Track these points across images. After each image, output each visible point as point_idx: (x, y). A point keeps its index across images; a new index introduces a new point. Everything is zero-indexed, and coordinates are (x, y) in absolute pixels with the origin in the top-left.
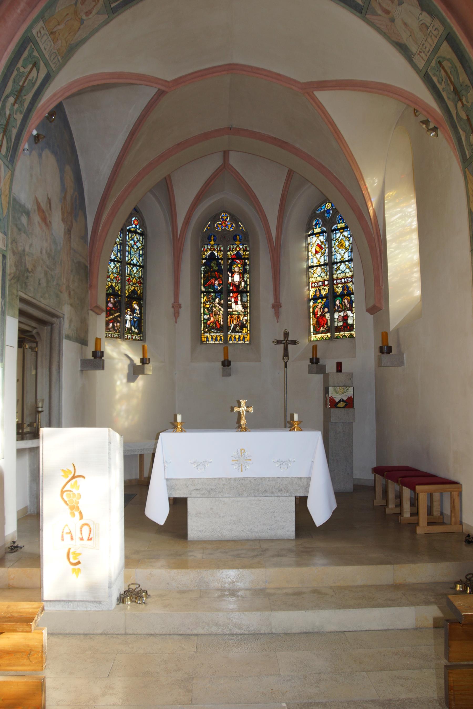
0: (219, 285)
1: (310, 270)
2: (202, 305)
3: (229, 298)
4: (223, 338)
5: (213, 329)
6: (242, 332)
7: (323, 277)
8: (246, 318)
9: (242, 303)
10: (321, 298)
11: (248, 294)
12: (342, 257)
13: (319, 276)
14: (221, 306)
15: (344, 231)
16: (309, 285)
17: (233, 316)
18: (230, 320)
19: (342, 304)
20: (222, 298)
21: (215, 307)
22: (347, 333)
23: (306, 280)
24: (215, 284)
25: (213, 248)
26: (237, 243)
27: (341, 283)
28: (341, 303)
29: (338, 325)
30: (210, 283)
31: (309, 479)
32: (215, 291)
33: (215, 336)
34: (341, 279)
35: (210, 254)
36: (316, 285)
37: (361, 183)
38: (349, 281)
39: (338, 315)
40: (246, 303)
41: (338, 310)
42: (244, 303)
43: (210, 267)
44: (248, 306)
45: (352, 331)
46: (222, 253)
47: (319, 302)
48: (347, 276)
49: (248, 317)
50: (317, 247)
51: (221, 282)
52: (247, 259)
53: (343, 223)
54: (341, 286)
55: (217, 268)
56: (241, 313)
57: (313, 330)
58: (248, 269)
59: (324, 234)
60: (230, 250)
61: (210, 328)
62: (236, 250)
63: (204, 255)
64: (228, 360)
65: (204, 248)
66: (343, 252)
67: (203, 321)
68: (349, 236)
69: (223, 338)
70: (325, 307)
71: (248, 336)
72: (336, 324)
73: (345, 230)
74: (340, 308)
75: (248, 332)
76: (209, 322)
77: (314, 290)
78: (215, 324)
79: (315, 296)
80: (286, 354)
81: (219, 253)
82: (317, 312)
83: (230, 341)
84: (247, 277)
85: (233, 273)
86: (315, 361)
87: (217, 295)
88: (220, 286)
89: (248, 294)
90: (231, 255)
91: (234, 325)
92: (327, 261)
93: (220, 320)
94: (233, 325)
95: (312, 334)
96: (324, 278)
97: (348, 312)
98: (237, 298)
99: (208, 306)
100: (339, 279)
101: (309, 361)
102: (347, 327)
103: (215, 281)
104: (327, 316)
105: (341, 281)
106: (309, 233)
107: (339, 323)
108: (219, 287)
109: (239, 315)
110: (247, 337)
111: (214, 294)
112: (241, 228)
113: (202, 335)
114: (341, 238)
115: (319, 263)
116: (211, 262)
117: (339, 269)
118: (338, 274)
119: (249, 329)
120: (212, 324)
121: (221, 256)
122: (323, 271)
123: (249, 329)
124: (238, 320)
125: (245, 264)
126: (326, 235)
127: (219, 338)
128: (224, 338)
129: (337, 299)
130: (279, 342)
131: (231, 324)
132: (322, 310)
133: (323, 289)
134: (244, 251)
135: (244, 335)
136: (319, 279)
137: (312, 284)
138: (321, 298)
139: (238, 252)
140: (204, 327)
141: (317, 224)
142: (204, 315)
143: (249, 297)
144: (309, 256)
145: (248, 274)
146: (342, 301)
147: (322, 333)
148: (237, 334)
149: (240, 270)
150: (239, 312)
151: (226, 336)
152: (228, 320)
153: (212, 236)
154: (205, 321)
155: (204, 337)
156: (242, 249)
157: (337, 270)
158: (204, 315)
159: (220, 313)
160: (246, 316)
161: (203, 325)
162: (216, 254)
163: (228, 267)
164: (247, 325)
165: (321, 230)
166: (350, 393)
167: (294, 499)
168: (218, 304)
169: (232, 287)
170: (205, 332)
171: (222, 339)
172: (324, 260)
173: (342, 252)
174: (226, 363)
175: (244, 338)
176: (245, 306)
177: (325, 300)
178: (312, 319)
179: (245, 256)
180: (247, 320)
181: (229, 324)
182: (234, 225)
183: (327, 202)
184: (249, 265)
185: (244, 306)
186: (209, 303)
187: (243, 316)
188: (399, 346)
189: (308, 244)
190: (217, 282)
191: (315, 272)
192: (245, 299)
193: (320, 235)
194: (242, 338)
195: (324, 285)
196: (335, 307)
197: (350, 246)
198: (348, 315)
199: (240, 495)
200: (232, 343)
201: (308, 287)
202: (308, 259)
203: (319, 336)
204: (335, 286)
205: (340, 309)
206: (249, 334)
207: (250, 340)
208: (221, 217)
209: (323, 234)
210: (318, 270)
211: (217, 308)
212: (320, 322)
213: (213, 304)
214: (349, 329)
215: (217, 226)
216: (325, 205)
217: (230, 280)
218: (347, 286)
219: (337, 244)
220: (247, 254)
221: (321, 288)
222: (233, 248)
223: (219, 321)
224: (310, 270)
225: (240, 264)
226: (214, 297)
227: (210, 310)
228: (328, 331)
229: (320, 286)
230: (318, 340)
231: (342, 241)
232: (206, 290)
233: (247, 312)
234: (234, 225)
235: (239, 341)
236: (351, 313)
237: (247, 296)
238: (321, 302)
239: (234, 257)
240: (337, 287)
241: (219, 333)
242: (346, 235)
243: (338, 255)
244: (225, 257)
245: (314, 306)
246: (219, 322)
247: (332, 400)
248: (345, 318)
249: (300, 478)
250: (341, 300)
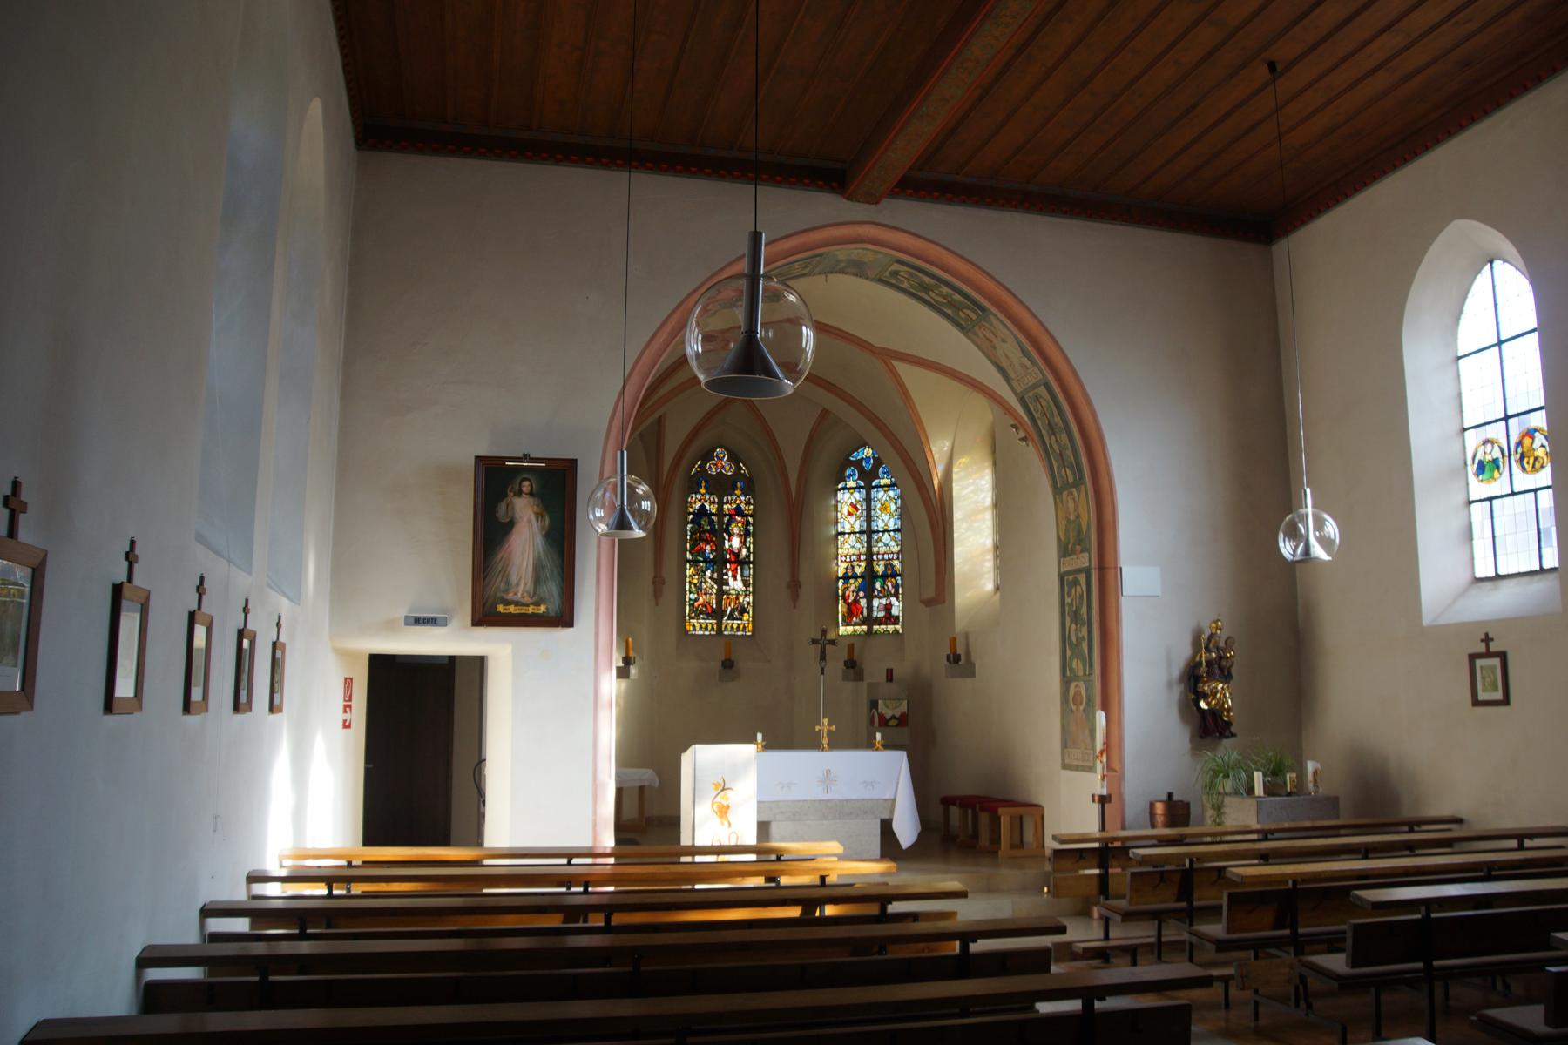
0: (712, 552)
1: (839, 537)
2: (688, 580)
3: (724, 571)
4: (715, 627)
5: (702, 613)
8: (747, 599)
10: (855, 577)
11: (751, 566)
12: (886, 525)
13: (853, 547)
15: (889, 490)
16: (837, 559)
21: (705, 582)
22: (891, 628)
27: (883, 559)
28: (882, 586)
31: (894, 800)
32: (706, 561)
35: (700, 507)
37: (927, 450)
43: (700, 525)
45: (898, 624)
49: (750, 599)
51: (714, 548)
52: (751, 516)
55: (709, 528)
57: (843, 620)
60: (727, 503)
62: (735, 503)
64: (730, 660)
69: (715, 627)
70: (859, 590)
71: (750, 625)
72: (875, 614)
76: (696, 604)
77: (844, 565)
78: (706, 606)
79: (846, 573)
80: (823, 657)
82: (849, 596)
85: (731, 535)
86: (851, 664)
89: (751, 566)
90: (728, 509)
92: (865, 528)
95: (841, 625)
99: (695, 581)
101: (843, 663)
102: (889, 618)
104: (863, 602)
106: (840, 486)
109: (738, 594)
114: (884, 498)
117: (881, 541)
121: (714, 511)
122: (859, 541)
125: (748, 522)
126: (864, 491)
127: (710, 627)
130: (814, 642)
132: (855, 594)
134: (746, 504)
136: (852, 551)
137: (842, 556)
138: (855, 577)
139: (738, 505)
140: (690, 610)
141: (851, 475)
146: (885, 583)
147: (855, 624)
149: (740, 531)
151: (719, 624)
154: (691, 602)
157: (877, 541)
158: (690, 593)
161: (688, 608)
162: (708, 507)
166: (904, 708)
167: (878, 822)
168: (710, 578)
170: (691, 618)
173: (886, 517)
174: (728, 664)
175: (744, 627)
177: (860, 580)
180: (748, 603)
182: (733, 467)
186: (697, 577)
188: (968, 653)
189: (837, 502)
190: (708, 548)
192: (746, 573)
194: (741, 627)
195: (859, 560)
199: (825, 818)
202: (837, 522)
203: (850, 629)
204: (875, 563)
207: (753, 631)
212: (852, 609)
215: (710, 467)
217: (727, 545)
218: (891, 564)
219: (879, 506)
224: (839, 537)
227: (699, 588)
228: (863, 623)
231: (887, 503)
234: (733, 467)
239: (733, 512)
242: (892, 496)
243: (880, 521)
244: (720, 513)
247: (881, 717)
248: (888, 608)
249: (886, 800)
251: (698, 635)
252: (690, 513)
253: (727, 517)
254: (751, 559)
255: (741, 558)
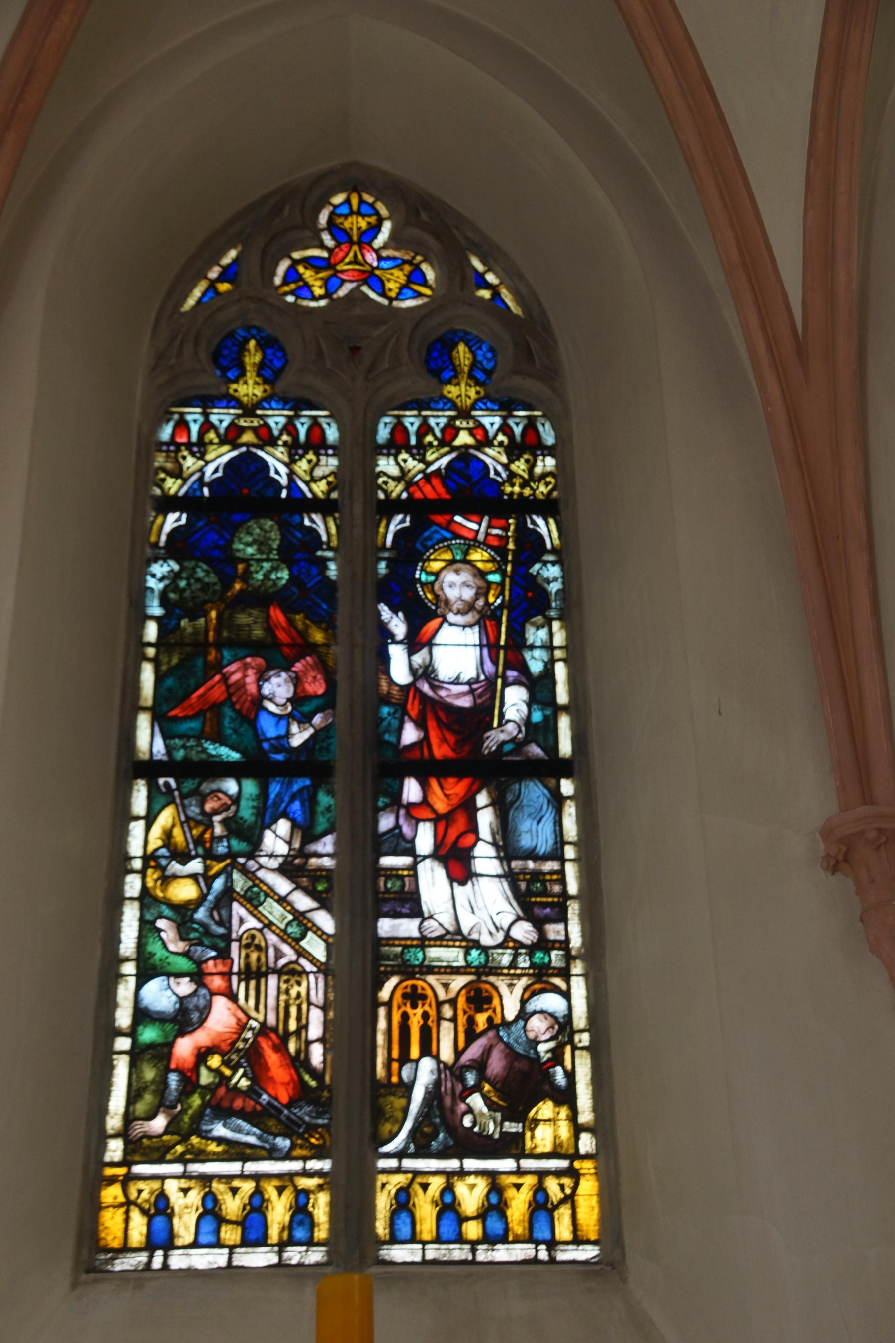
2: (133, 885)
3: (386, 822)
5: (224, 1113)
6: (520, 1136)
9: (516, 864)
14: (311, 893)
17: (431, 979)
18: (396, 1017)
20: (322, 823)
21: (252, 901)
24: (259, 700)
25: (255, 430)
26: (452, 391)
30: (218, 693)
33: (248, 1187)
40: (551, 866)
42: (531, 865)
44: (573, 888)
46: (333, 462)
51: (316, 687)
52: (548, 508)
55: (284, 575)
56: (506, 959)
58: (554, 587)
61: (196, 1101)
63: (178, 473)
65: (182, 425)
67: (132, 1033)
71: (588, 1187)
75: (587, 1143)
76: (184, 1048)
81: (302, 466)
83: (394, 1239)
84: (549, 647)
87: (275, 789)
88: (305, 719)
89: (567, 787)
90: (402, 477)
91: (442, 1067)
93: (303, 1027)
94: (426, 1070)
98: (461, 823)
99: (184, 891)
103: (262, 677)
108: (295, 728)
110: (570, 1199)
111: (250, 787)
112: (486, 294)
113: (112, 1180)
116: (233, 529)
119: (586, 1116)
120: (215, 1061)
121: (320, 488)
123: (586, 1116)
124: (481, 1019)
128: (332, 1204)
131: (405, 1058)
134: (513, 450)
135: (542, 1175)
140: (133, 1097)
142: (142, 978)
143: (570, 812)
145: (556, 625)
148: (471, 1164)
149: (483, 591)
150: (485, 949)
152: (382, 1024)
153: (252, 344)
154: (149, 1034)
155: (128, 1203)
156: (501, 437)
158: (143, 977)
159: (302, 953)
160: (558, 982)
163: (382, 566)
164: (571, 1076)
168: (287, 869)
169: (420, 724)
171: (312, 1225)
176: (545, 893)
179: (524, 484)
181: (389, 1060)
184: (561, 556)
185: (529, 893)
186: (195, 866)
187: (524, 981)
200: (424, 1262)
206: (586, 1167)
208: (323, 218)
211: (278, 909)
213: (236, 876)
215: (292, 275)
217: (400, 672)
220: (538, 470)
222: (425, 429)
223: (287, 1035)
225: (486, 545)
226: (246, 812)
232: (180, 754)
233: (564, 945)
234: (430, 274)
235: (489, 1239)
237: (558, 801)
239: (434, 491)
241: (288, 1156)
246: (292, 1046)
251: (191, 1273)
252: (167, 504)
253: (401, 521)
254: (565, 747)
255: (494, 738)
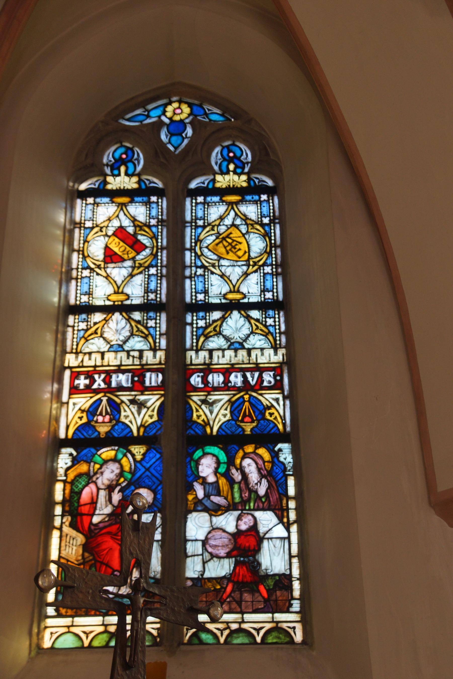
1: (71, 320)
7: (136, 354)
15: (243, 201)
16: (60, 381)
19: (227, 475)
23: (52, 354)
29: (207, 575)
34: (226, 372)
36: (99, 383)
38: (265, 384)
39: (208, 524)
41: (207, 503)
47: (104, 456)
48: (257, 364)
50: (117, 240)
53: (242, 173)
54: (226, 398)
59: (154, 199)
66: (238, 271)
68: (266, 221)
73: (248, 198)
74: (218, 494)
82: (93, 502)
96: (141, 357)
97: (258, 514)
100: (217, 371)
105: (227, 381)
106: (83, 187)
107: (210, 565)
114: (228, 221)
115: (122, 297)
117: (219, 333)
118: (211, 352)
129: (205, 454)
132: (116, 497)
133: (133, 402)
137: (75, 376)
144: (74, 266)
146: (231, 462)
165: (139, 182)
172: (147, 291)
178: (56, 534)
183: (174, 99)
191: (96, 332)
193: (132, 201)
196: (190, 488)
197: (270, 254)
198: (262, 529)
201: (56, 386)
204: (196, 398)
205: (216, 499)
209: (145, 199)
210: (112, 324)
214: (266, 601)
216: (166, 105)
218: (255, 402)
221: (125, 397)
224: (71, 320)
229: (121, 388)
230: (83, 647)
231: (235, 234)
236: (275, 520)
238: (115, 460)
240: (204, 402)
243: (215, 280)
245: (80, 475)
250: (223, 457)
